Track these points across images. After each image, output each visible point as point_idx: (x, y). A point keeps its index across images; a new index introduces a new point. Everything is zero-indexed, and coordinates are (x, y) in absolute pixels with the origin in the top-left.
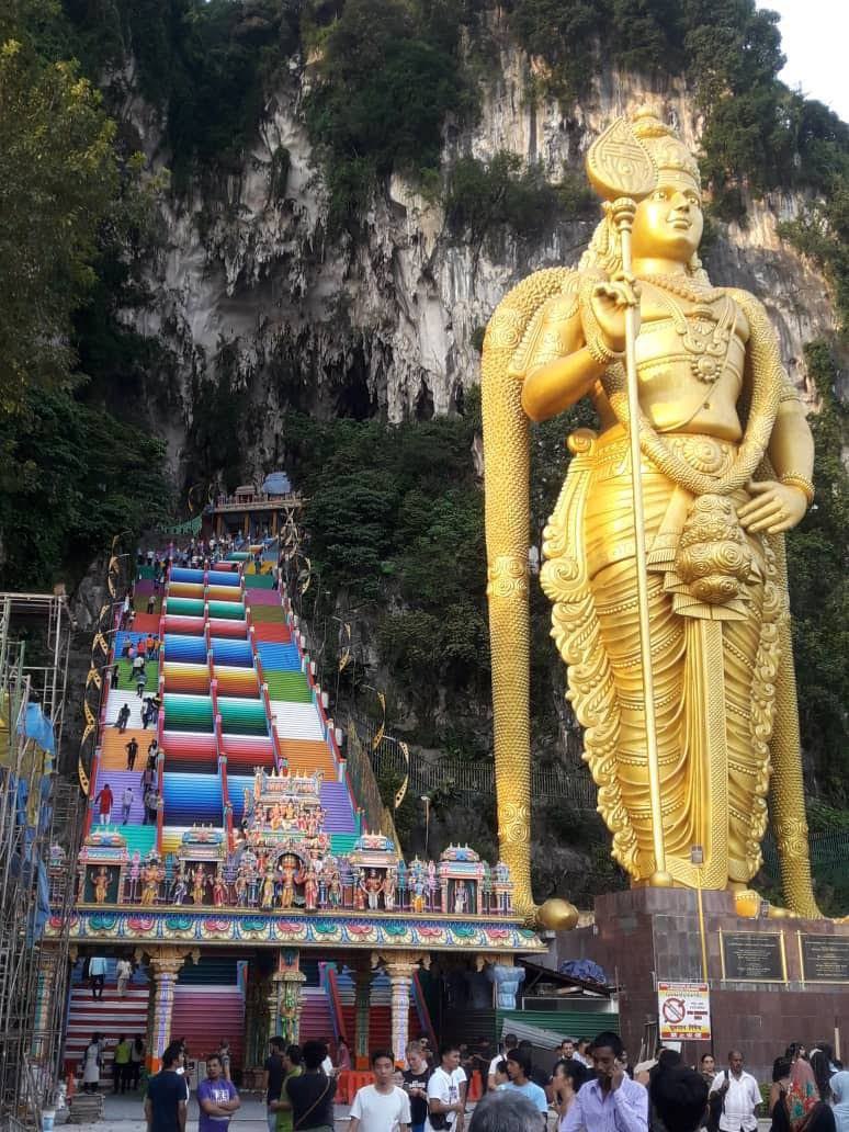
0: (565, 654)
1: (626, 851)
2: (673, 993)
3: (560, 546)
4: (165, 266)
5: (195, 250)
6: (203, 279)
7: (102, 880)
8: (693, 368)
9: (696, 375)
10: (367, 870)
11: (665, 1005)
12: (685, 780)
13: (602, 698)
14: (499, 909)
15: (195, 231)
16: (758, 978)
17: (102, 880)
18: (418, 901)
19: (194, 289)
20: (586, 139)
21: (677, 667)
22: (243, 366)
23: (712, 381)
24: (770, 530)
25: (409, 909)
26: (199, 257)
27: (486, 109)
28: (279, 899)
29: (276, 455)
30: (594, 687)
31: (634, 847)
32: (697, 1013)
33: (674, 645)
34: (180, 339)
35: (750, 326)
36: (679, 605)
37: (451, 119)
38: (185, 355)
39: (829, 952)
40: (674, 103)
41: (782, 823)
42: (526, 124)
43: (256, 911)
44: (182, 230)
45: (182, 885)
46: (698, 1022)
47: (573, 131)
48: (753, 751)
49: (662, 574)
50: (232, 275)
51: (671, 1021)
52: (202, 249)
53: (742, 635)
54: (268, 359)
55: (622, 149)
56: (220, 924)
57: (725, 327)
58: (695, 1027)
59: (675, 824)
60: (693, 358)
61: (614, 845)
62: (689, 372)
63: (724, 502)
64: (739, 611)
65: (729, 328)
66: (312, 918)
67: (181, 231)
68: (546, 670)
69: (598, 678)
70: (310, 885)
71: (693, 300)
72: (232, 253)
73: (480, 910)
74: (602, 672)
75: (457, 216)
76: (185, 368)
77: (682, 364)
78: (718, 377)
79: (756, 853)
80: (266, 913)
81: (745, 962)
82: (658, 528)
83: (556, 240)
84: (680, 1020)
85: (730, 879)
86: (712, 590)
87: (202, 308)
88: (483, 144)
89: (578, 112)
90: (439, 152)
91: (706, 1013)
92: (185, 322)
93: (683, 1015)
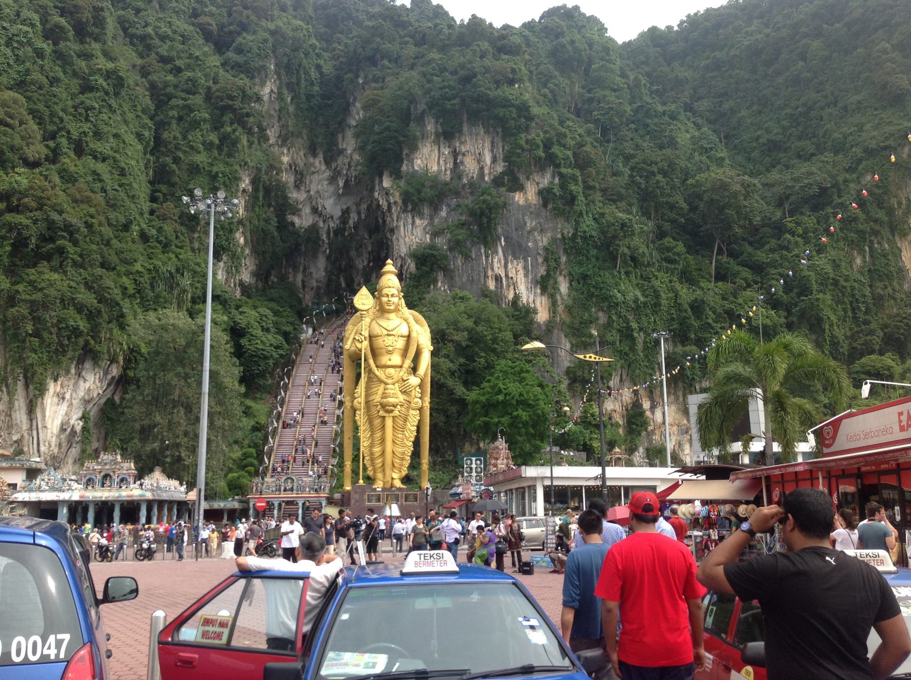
0: (359, 423)
4: (311, 182)
5: (324, 172)
6: (330, 183)
20: (460, 157)
21: (383, 427)
22: (351, 222)
26: (327, 174)
27: (420, 146)
29: (369, 262)
34: (320, 215)
36: (382, 413)
37: (405, 151)
38: (324, 222)
42: (436, 151)
44: (318, 163)
47: (455, 154)
50: (341, 184)
54: (363, 216)
64: (396, 413)
67: (317, 164)
68: (356, 428)
72: (339, 173)
75: (407, 198)
83: (444, 208)
87: (330, 197)
88: (419, 161)
89: (458, 144)
90: (401, 166)
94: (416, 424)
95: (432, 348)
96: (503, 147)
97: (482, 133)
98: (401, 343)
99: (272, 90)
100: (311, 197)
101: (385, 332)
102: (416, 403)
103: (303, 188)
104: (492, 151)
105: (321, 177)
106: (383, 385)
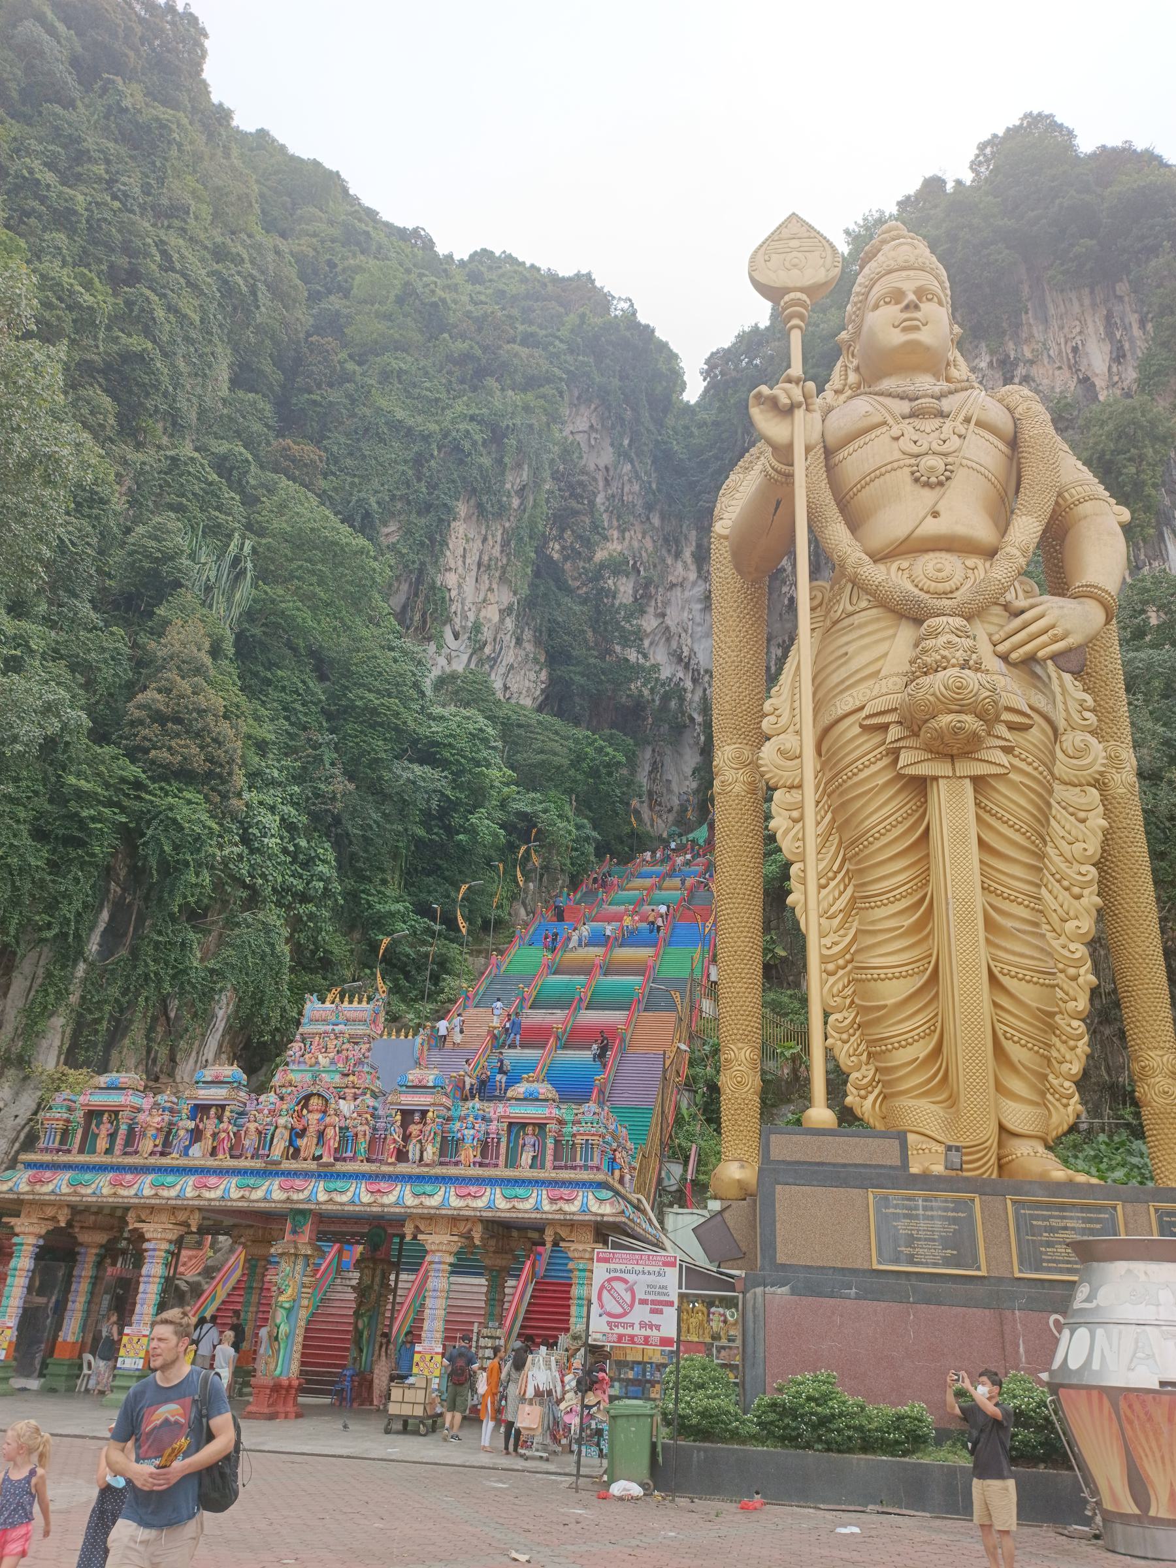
1: (865, 1098)
2: (618, 1267)
3: (784, 720)
4: (666, 604)
5: (694, 584)
7: (105, 1129)
8: (913, 473)
9: (917, 480)
10: (405, 1113)
11: (602, 1287)
12: (937, 993)
13: (835, 900)
14: (578, 1162)
15: (693, 567)
16: (935, 1265)
17: (105, 1129)
18: (469, 1153)
19: (698, 619)
23: (941, 484)
24: (1040, 654)
25: (457, 1164)
28: (297, 1151)
30: (824, 887)
31: (877, 1091)
32: (653, 1302)
33: (917, 815)
35: (1016, 421)
36: (913, 762)
39: (1065, 1228)
40: (1117, 309)
41: (1137, 1060)
43: (258, 1164)
45: (182, 1133)
46: (656, 1319)
48: (1050, 954)
49: (885, 727)
51: (610, 1315)
52: (700, 582)
53: (1015, 797)
55: (794, 243)
56: (212, 1180)
57: (961, 417)
58: (651, 1326)
59: (922, 1056)
60: (913, 461)
61: (849, 1087)
62: (908, 479)
63: (958, 622)
65: (967, 420)
66: (326, 1174)
69: (830, 874)
70: (330, 1132)
71: (911, 400)
73: (548, 1164)
74: (835, 868)
76: (693, 692)
77: (899, 472)
78: (948, 479)
79: (1070, 1097)
80: (274, 1167)
81: (911, 1240)
82: (879, 671)
84: (625, 1314)
85: (1002, 1128)
86: (940, 735)
89: (1011, 345)
91: (671, 1304)
92: (691, 650)
93: (632, 1306)
94: (1093, 847)
95: (1125, 514)
96: (1142, 324)
97: (1076, 308)
98: (984, 452)
99: (592, 426)
100: (667, 628)
101: (905, 407)
102: (1081, 752)
103: (651, 610)
104: (1110, 335)
105: (687, 594)
106: (906, 633)
